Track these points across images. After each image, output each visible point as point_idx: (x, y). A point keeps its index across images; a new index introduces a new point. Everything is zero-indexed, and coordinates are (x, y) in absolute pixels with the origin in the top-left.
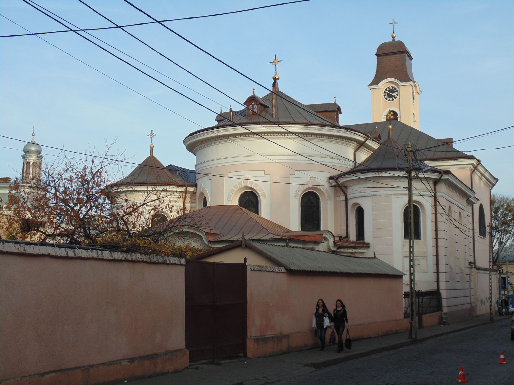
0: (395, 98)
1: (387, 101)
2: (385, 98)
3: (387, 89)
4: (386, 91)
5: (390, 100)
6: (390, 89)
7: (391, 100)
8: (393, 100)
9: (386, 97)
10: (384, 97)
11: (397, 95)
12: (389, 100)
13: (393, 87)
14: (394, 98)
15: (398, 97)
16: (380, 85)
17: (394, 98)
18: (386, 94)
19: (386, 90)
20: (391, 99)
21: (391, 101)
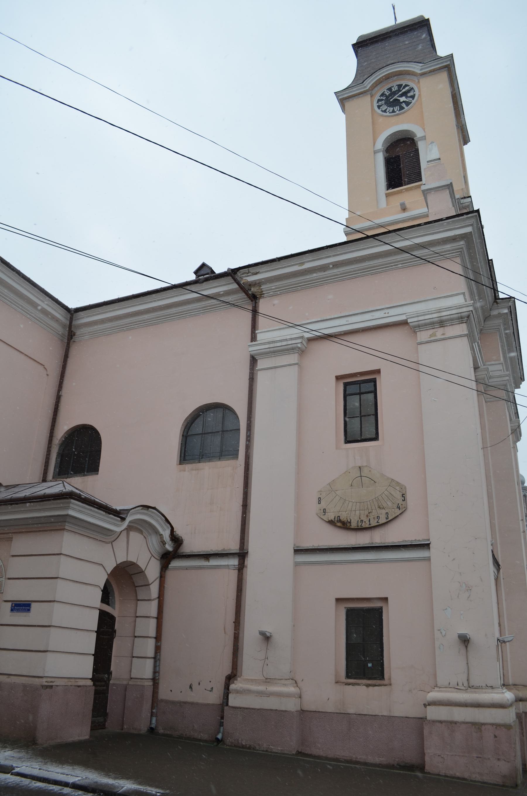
0: (408, 104)
1: (388, 114)
2: (382, 111)
3: (386, 93)
4: (382, 98)
5: (393, 111)
6: (393, 90)
7: (395, 110)
8: (402, 108)
9: (384, 107)
10: (379, 108)
11: (413, 97)
12: (391, 111)
13: (400, 86)
14: (404, 105)
15: (413, 101)
16: (369, 83)
17: (404, 105)
18: (383, 102)
19: (383, 95)
20: (396, 108)
21: (397, 112)
